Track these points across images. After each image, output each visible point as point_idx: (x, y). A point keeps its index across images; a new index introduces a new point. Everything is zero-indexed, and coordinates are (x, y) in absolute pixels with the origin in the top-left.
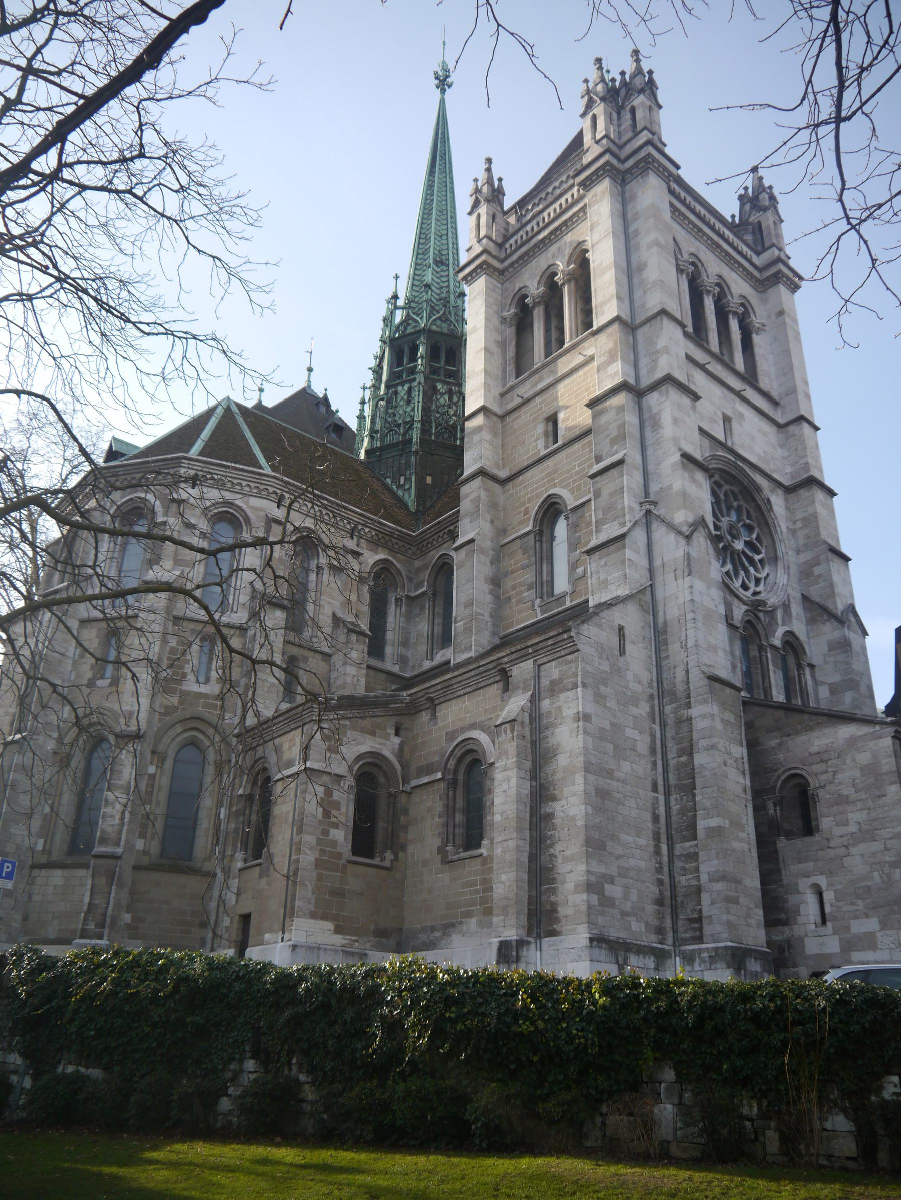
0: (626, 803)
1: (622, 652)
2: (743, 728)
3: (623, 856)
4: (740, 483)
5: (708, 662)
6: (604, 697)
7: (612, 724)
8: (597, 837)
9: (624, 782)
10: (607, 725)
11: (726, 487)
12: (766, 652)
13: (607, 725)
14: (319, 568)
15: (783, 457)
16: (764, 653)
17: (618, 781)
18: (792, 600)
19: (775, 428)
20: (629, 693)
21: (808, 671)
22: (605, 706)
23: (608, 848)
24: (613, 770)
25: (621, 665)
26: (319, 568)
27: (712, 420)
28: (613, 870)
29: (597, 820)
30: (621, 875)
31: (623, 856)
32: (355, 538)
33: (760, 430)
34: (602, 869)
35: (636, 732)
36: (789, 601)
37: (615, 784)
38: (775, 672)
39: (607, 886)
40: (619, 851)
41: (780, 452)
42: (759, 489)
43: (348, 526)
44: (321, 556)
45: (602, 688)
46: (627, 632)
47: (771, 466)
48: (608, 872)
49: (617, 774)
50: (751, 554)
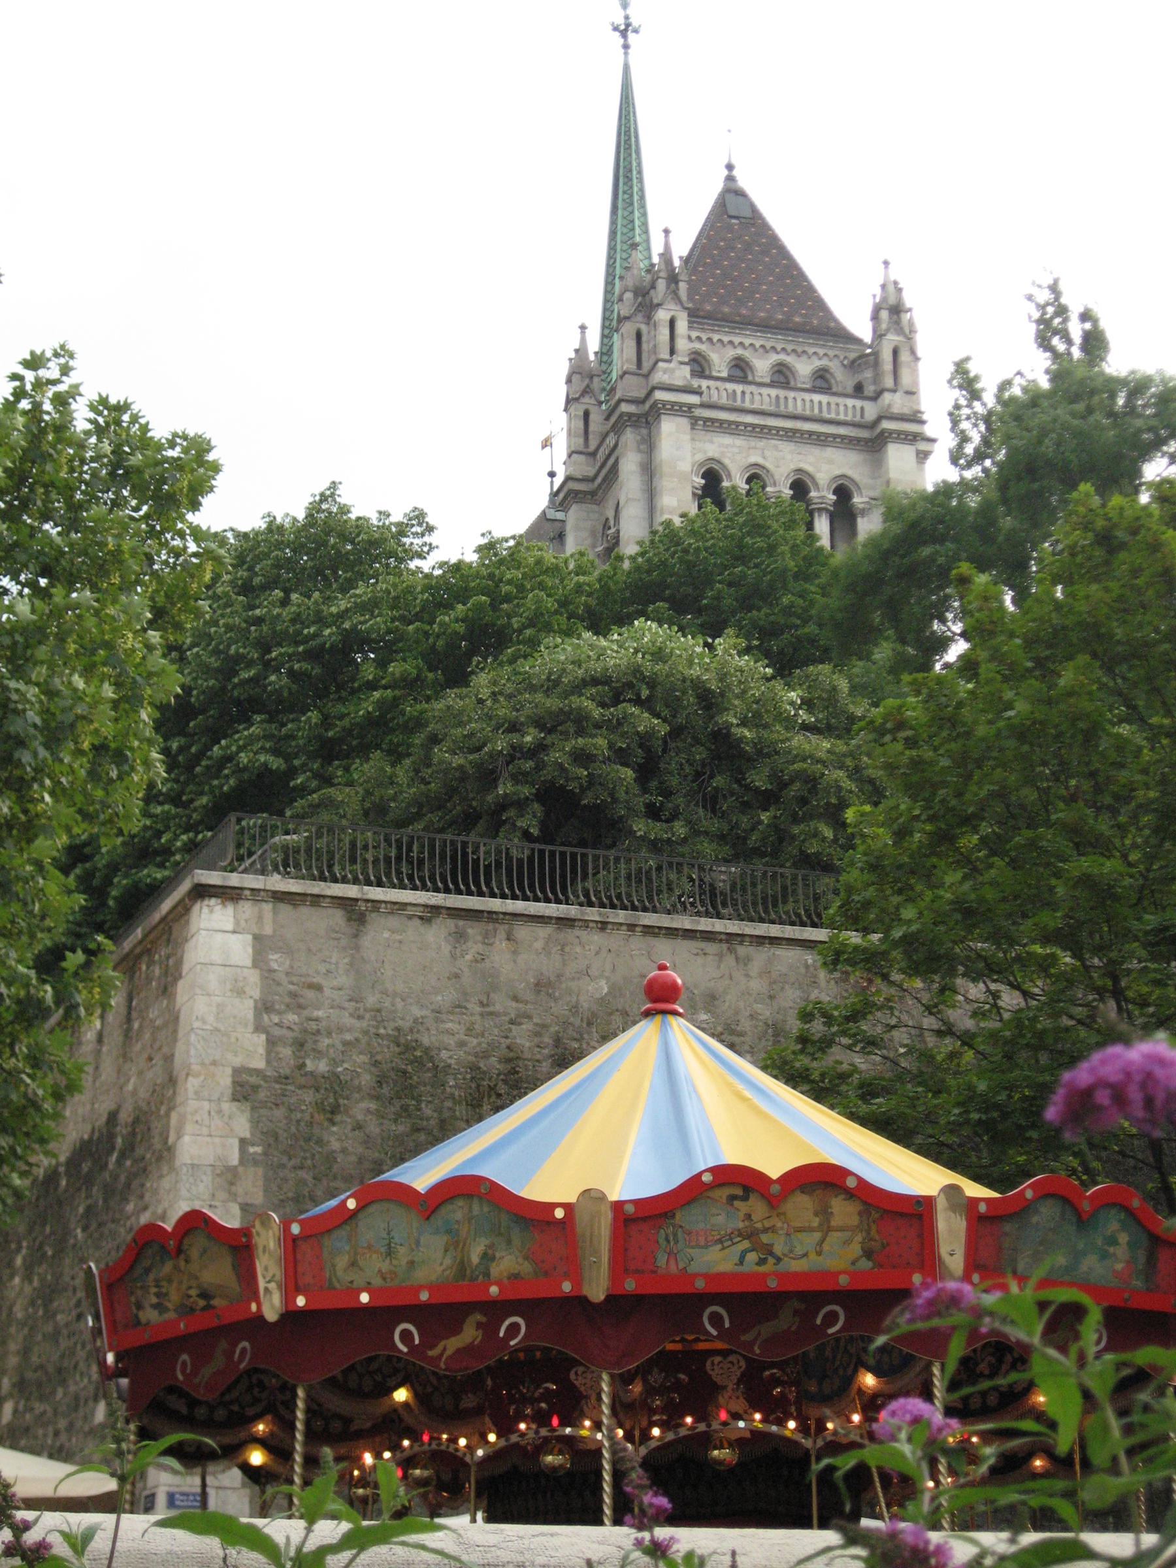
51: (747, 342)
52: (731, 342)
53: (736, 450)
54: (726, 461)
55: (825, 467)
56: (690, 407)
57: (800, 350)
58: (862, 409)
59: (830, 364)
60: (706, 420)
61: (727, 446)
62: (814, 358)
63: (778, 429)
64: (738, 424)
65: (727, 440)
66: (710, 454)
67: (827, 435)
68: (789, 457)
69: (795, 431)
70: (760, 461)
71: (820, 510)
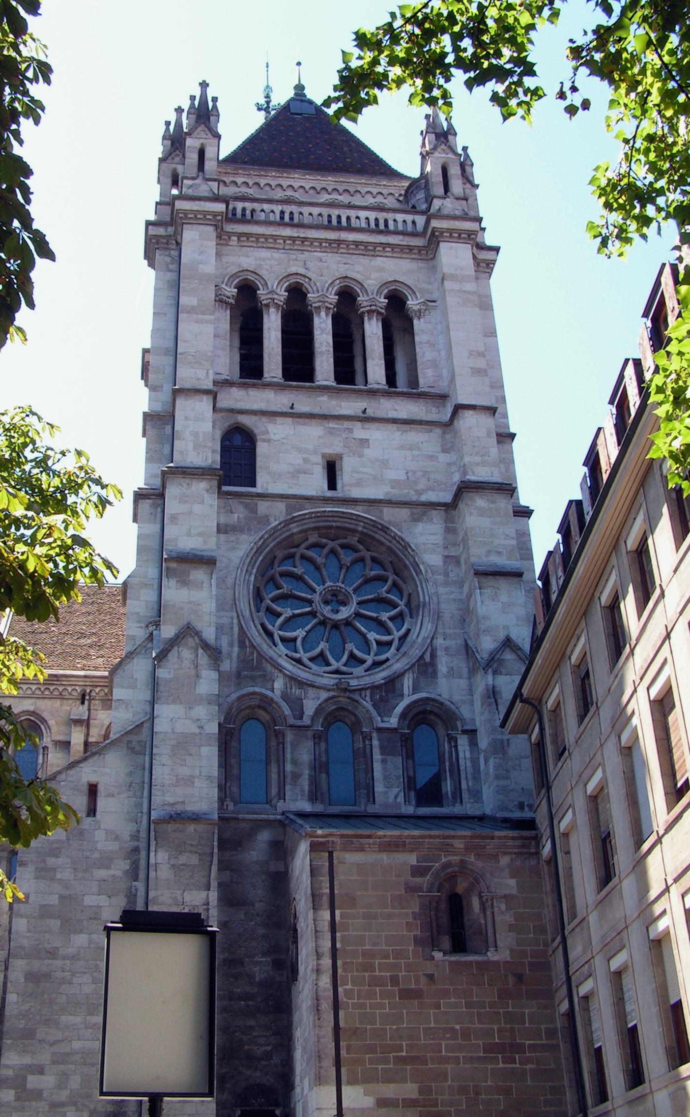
0: (75, 980)
1: (92, 811)
2: (214, 868)
3: (63, 1041)
4: (354, 531)
5: (171, 800)
6: (54, 870)
7: (61, 897)
8: (20, 1026)
9: (75, 958)
10: (54, 900)
11: (332, 544)
12: (371, 740)
13: (54, 900)
14: (45, 748)
15: (449, 465)
16: (367, 742)
17: (64, 958)
18: (439, 653)
19: (438, 431)
20: (96, 855)
21: (463, 742)
22: (52, 879)
23: (38, 1035)
24: (57, 948)
25: (87, 827)
26: (45, 748)
27: (298, 472)
28: (44, 1058)
29: (25, 1007)
30: (54, 1062)
31: (63, 1041)
32: (86, 702)
33: (402, 447)
34: (27, 1060)
35: (103, 897)
36: (433, 656)
37: (59, 963)
38: (383, 761)
39: (30, 1078)
40: (59, 1035)
41: (444, 458)
42: (385, 529)
43: (75, 693)
44: (45, 735)
45: (51, 861)
46: (101, 788)
47: (420, 487)
48: (35, 1062)
49: (62, 952)
50: (374, 615)
51: (296, 185)
52: (280, 186)
53: (273, 262)
54: (264, 273)
55: (375, 275)
56: (215, 214)
57: (352, 190)
58: (414, 222)
59: (385, 201)
60: (240, 235)
61: (264, 260)
62: (369, 196)
63: (321, 241)
64: (275, 238)
65: (264, 254)
66: (245, 267)
67: (376, 245)
68: (334, 267)
69: (339, 242)
70: (301, 271)
71: (368, 312)
